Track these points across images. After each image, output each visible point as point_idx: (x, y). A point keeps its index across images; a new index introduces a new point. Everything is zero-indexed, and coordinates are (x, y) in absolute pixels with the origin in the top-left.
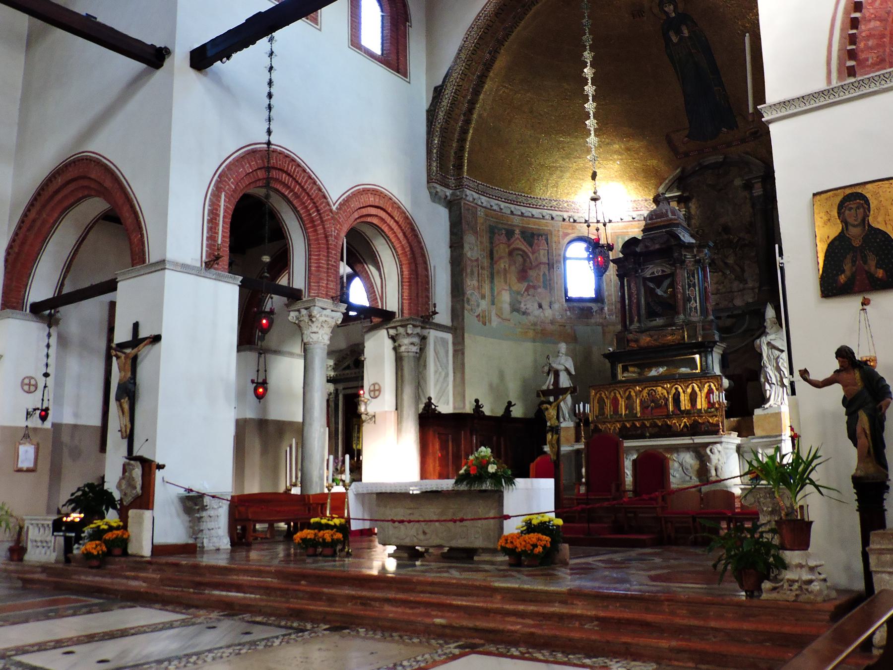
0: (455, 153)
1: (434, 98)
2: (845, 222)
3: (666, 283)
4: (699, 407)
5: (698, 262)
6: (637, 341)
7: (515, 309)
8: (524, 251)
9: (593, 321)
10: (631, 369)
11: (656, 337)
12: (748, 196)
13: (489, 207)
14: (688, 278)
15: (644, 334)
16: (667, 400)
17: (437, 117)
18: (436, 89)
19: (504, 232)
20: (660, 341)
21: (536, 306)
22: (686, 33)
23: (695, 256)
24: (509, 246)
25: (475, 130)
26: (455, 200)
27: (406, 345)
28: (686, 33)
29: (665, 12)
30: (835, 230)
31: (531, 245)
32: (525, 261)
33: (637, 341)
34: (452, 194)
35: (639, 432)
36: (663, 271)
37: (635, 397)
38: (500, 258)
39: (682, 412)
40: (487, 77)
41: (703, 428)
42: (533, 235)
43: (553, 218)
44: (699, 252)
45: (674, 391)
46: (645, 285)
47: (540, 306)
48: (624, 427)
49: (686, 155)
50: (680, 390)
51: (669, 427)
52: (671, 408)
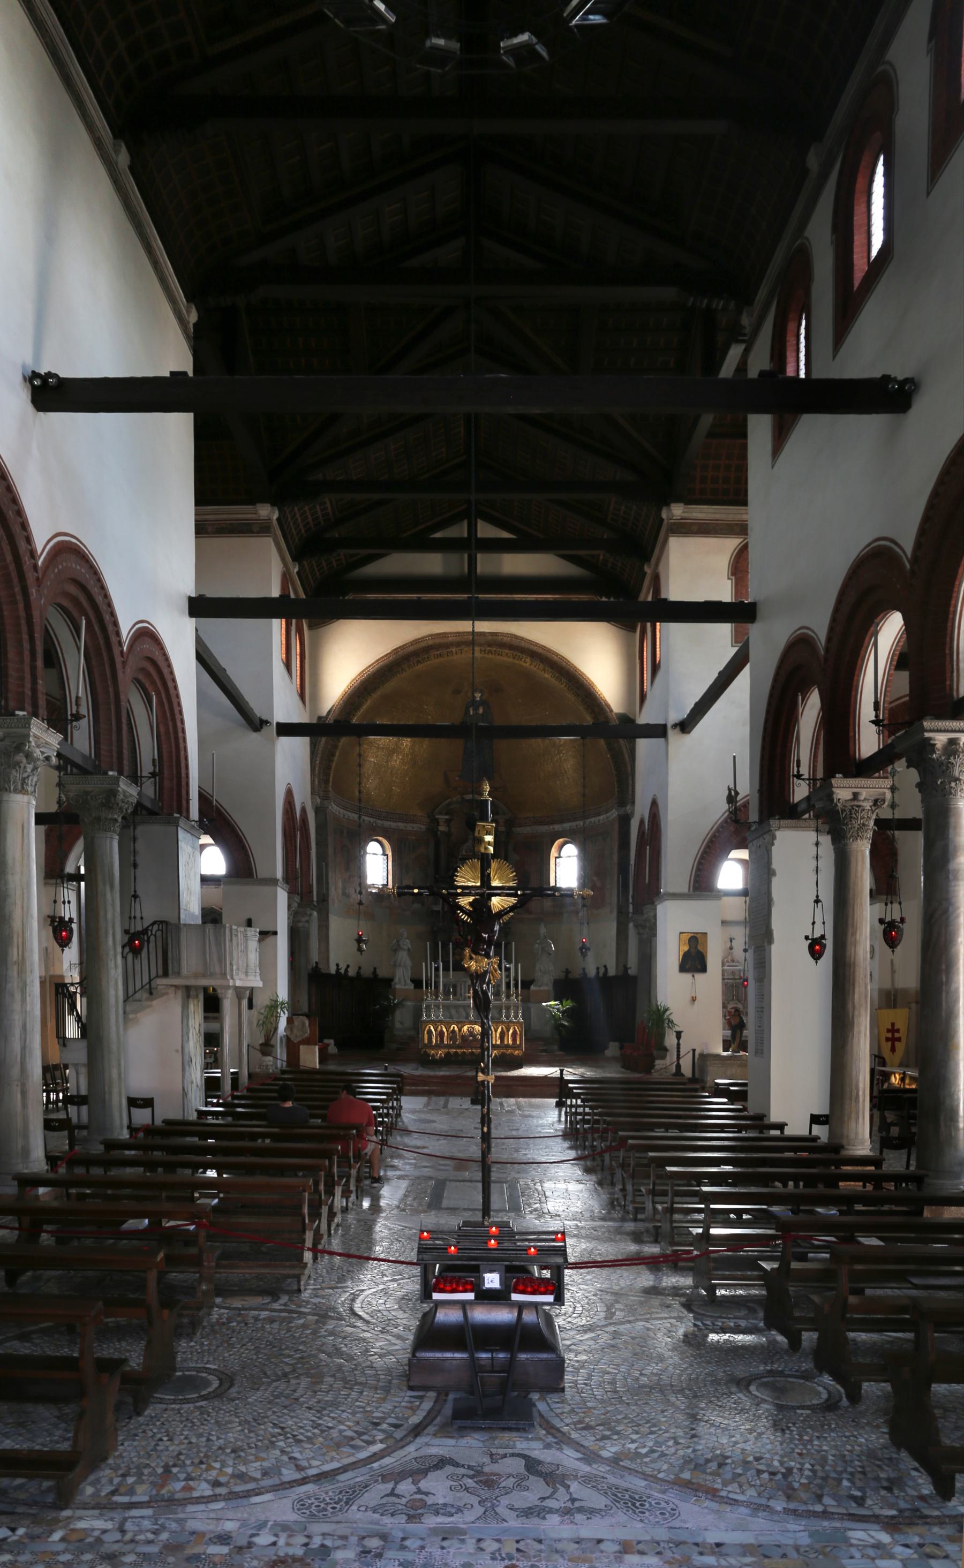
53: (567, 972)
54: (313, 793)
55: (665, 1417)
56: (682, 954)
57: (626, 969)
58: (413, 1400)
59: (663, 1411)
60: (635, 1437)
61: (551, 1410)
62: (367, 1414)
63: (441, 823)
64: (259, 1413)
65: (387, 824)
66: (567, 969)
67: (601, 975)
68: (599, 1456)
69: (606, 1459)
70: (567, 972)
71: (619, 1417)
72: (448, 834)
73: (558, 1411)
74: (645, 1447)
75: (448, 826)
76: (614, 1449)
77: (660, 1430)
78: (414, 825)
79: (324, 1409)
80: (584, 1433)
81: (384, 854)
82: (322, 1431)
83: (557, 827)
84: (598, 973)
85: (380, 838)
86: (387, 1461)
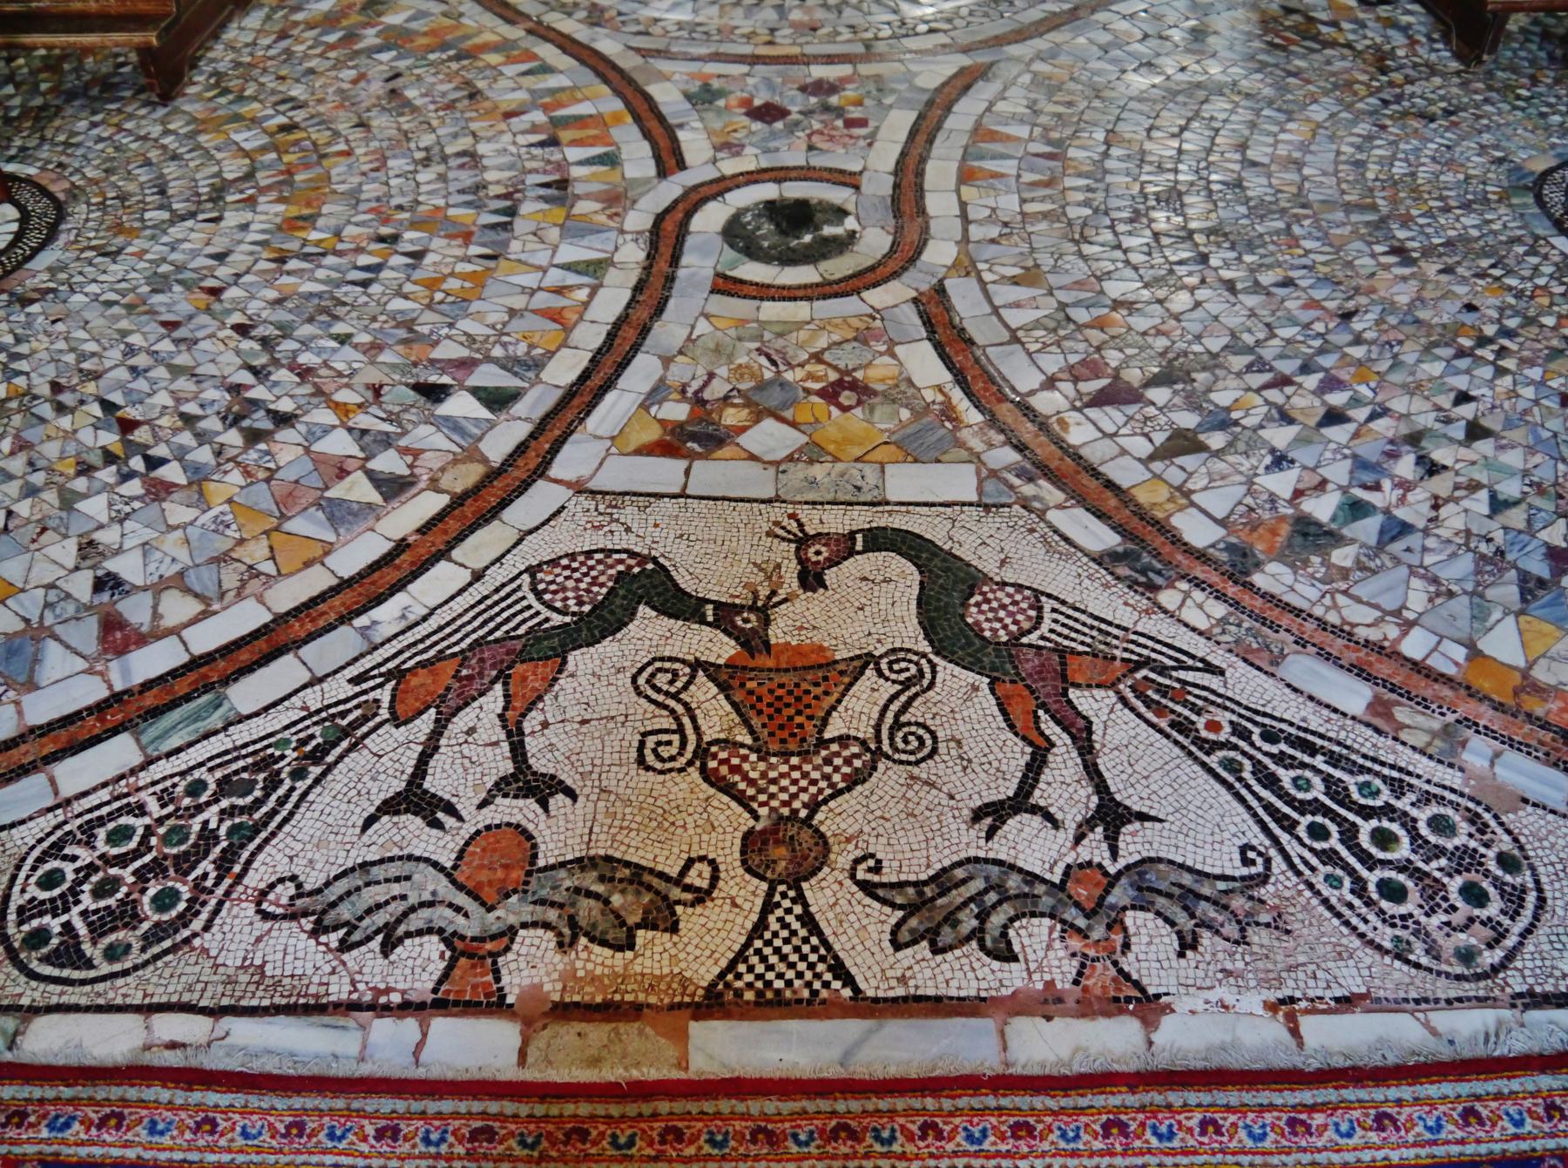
55: (1358, 340)
58: (572, 279)
59: (1347, 316)
60: (1281, 436)
61: (996, 310)
62: (417, 351)
64: (83, 357)
68: (1176, 540)
69: (1201, 556)
71: (1215, 344)
73: (1015, 318)
74: (1322, 485)
76: (1219, 502)
77: (1356, 401)
79: (286, 331)
80: (1110, 417)
82: (253, 437)
86: (441, 580)
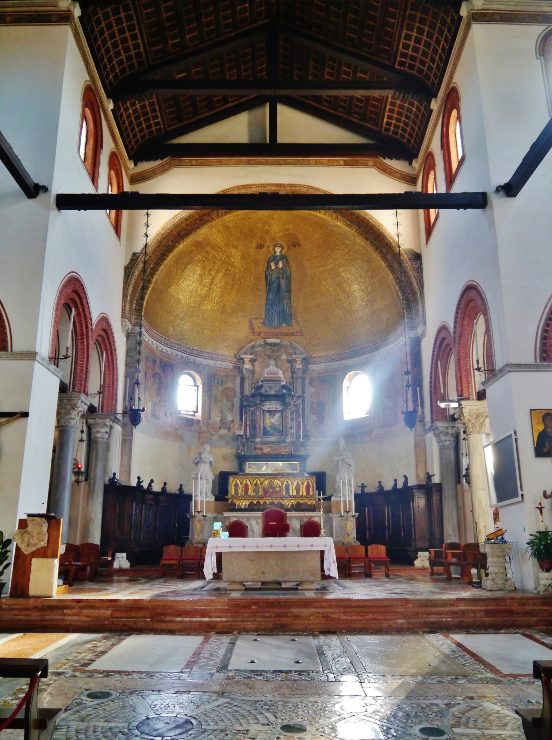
0: (137, 301)
1: (132, 260)
2: (545, 424)
3: (278, 415)
4: (301, 494)
5: (296, 406)
6: (261, 449)
7: (153, 415)
8: (159, 375)
9: (193, 428)
10: (253, 467)
11: (274, 448)
12: (290, 366)
13: (147, 341)
14: (291, 415)
15: (267, 446)
16: (280, 488)
17: (133, 273)
18: (134, 254)
19: (152, 360)
20: (277, 451)
21: (164, 414)
22: (280, 265)
23: (295, 402)
24: (153, 370)
25: (153, 288)
26: (132, 333)
27: (102, 433)
28: (280, 265)
29: (275, 252)
30: (541, 428)
31: (164, 372)
32: (160, 382)
33: (261, 449)
34: (132, 329)
35: (262, 507)
36: (276, 408)
37: (260, 485)
38: (149, 378)
39: (291, 497)
40: (167, 256)
41: (303, 507)
42: (165, 365)
43: (177, 355)
44: (297, 400)
45: (285, 483)
46: (263, 414)
47: (166, 415)
48: (251, 504)
49: (259, 334)
50: (290, 482)
51: (282, 505)
52: (284, 494)
53: (363, 486)
54: (123, 316)
56: (536, 435)
57: (429, 477)
63: (246, 361)
65: (199, 360)
66: (363, 484)
67: (400, 485)
70: (363, 486)
72: (253, 372)
75: (253, 365)
78: (223, 363)
81: (196, 385)
83: (348, 362)
84: (396, 484)
85: (192, 372)
